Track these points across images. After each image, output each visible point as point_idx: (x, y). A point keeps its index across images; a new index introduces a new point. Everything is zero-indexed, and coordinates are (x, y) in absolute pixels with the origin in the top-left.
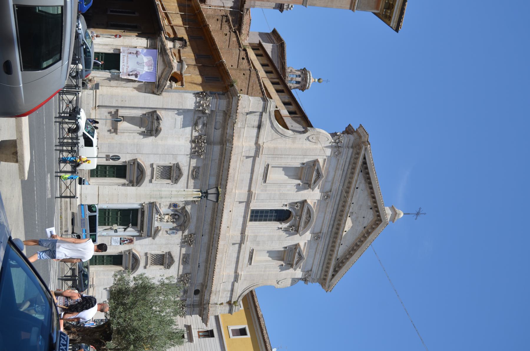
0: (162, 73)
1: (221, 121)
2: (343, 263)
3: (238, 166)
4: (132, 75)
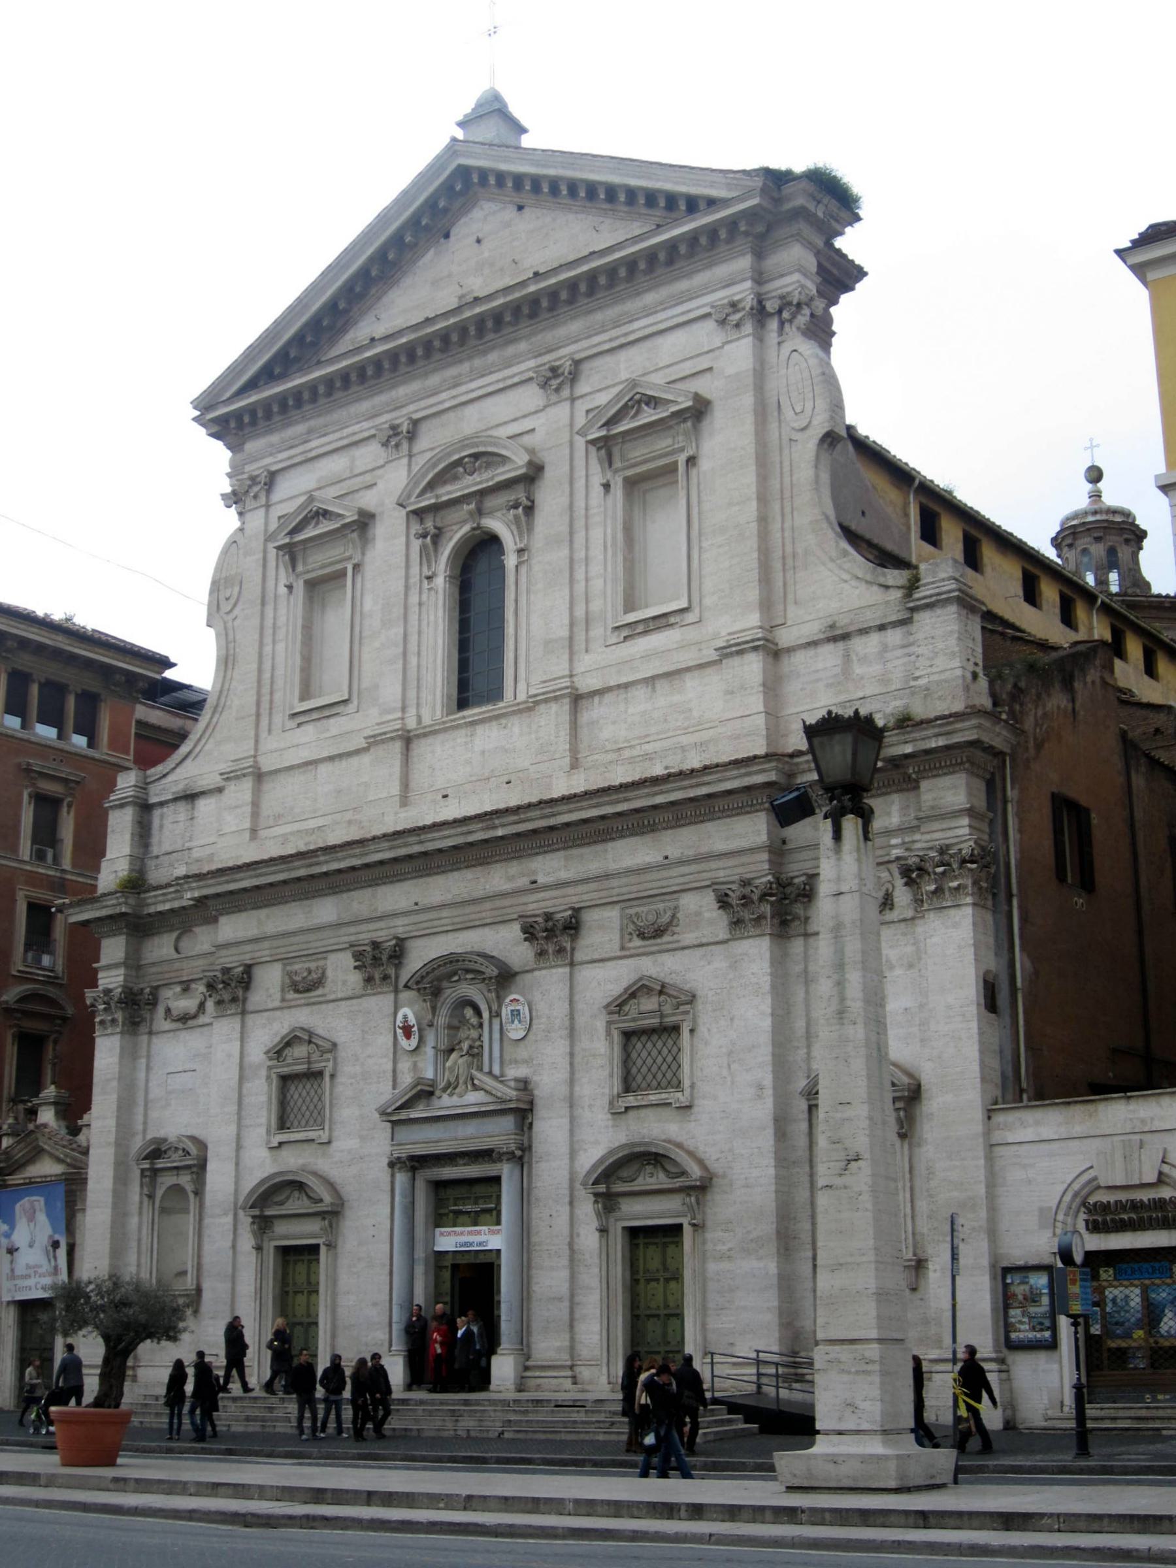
1: (175, 935)
2: (651, 198)
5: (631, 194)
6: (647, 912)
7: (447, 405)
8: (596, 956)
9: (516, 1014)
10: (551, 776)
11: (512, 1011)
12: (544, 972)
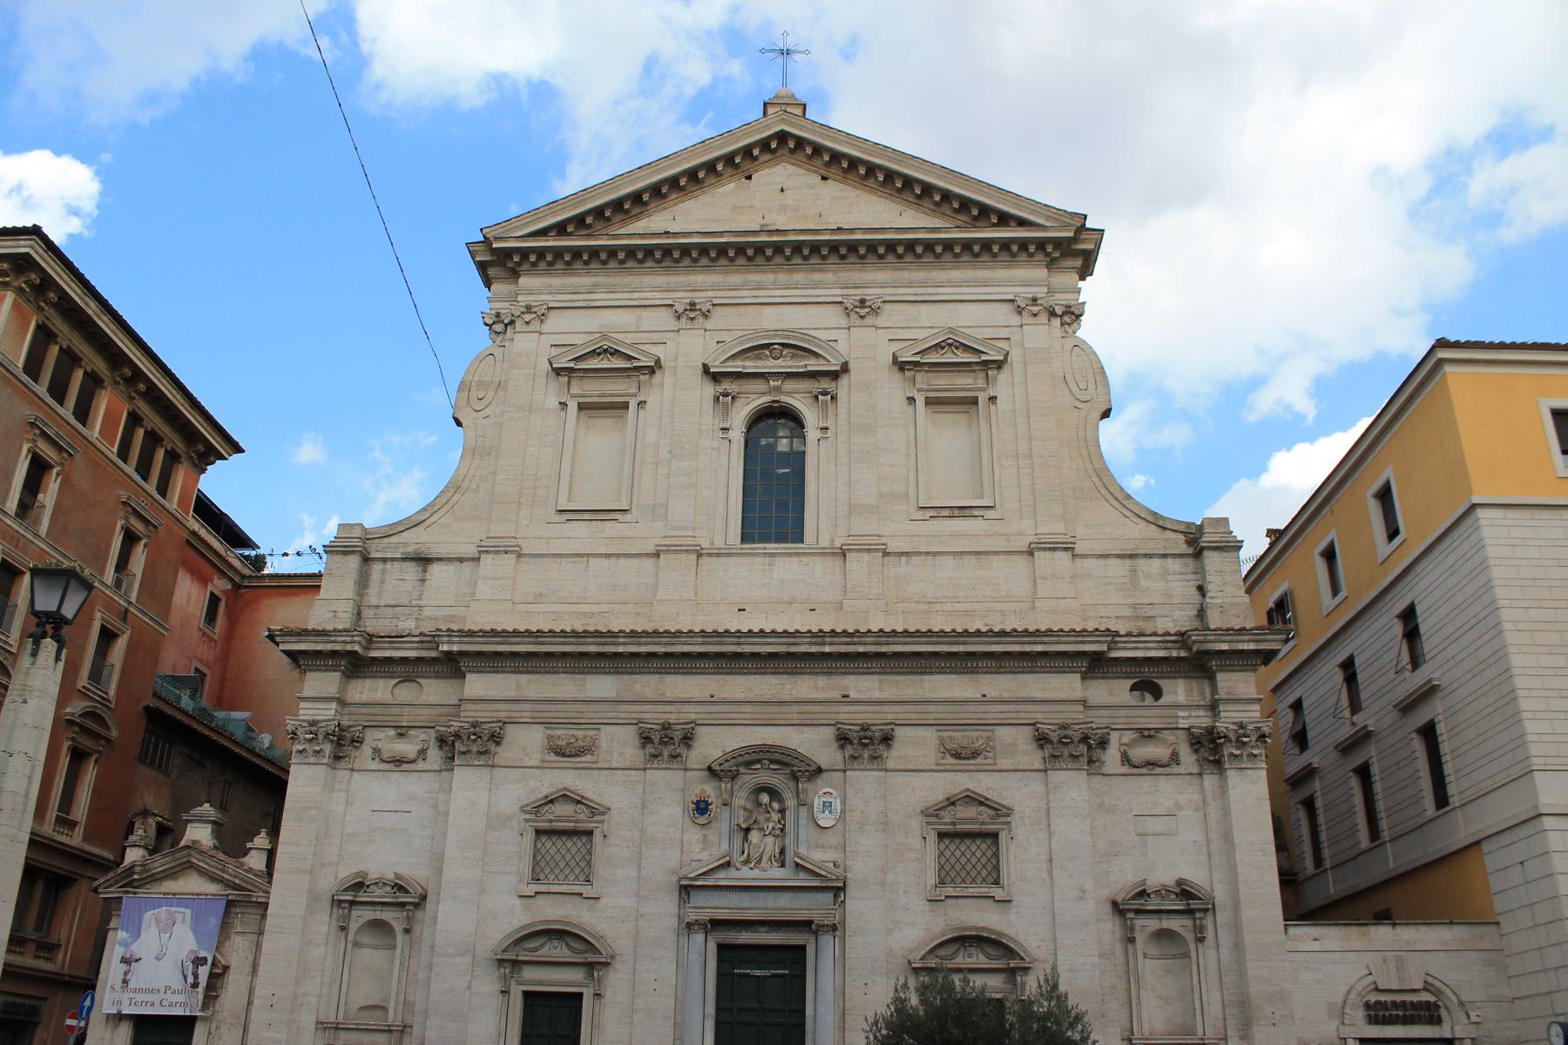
0: (213, 878)
1: (394, 681)
2: (965, 204)
3: (554, 608)
4: (196, 976)
5: (947, 196)
6: (960, 737)
7: (747, 301)
8: (910, 766)
9: (827, 806)
10: (868, 612)
11: (824, 802)
12: (857, 773)
